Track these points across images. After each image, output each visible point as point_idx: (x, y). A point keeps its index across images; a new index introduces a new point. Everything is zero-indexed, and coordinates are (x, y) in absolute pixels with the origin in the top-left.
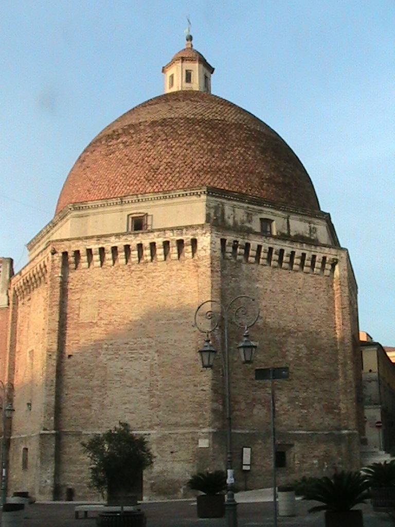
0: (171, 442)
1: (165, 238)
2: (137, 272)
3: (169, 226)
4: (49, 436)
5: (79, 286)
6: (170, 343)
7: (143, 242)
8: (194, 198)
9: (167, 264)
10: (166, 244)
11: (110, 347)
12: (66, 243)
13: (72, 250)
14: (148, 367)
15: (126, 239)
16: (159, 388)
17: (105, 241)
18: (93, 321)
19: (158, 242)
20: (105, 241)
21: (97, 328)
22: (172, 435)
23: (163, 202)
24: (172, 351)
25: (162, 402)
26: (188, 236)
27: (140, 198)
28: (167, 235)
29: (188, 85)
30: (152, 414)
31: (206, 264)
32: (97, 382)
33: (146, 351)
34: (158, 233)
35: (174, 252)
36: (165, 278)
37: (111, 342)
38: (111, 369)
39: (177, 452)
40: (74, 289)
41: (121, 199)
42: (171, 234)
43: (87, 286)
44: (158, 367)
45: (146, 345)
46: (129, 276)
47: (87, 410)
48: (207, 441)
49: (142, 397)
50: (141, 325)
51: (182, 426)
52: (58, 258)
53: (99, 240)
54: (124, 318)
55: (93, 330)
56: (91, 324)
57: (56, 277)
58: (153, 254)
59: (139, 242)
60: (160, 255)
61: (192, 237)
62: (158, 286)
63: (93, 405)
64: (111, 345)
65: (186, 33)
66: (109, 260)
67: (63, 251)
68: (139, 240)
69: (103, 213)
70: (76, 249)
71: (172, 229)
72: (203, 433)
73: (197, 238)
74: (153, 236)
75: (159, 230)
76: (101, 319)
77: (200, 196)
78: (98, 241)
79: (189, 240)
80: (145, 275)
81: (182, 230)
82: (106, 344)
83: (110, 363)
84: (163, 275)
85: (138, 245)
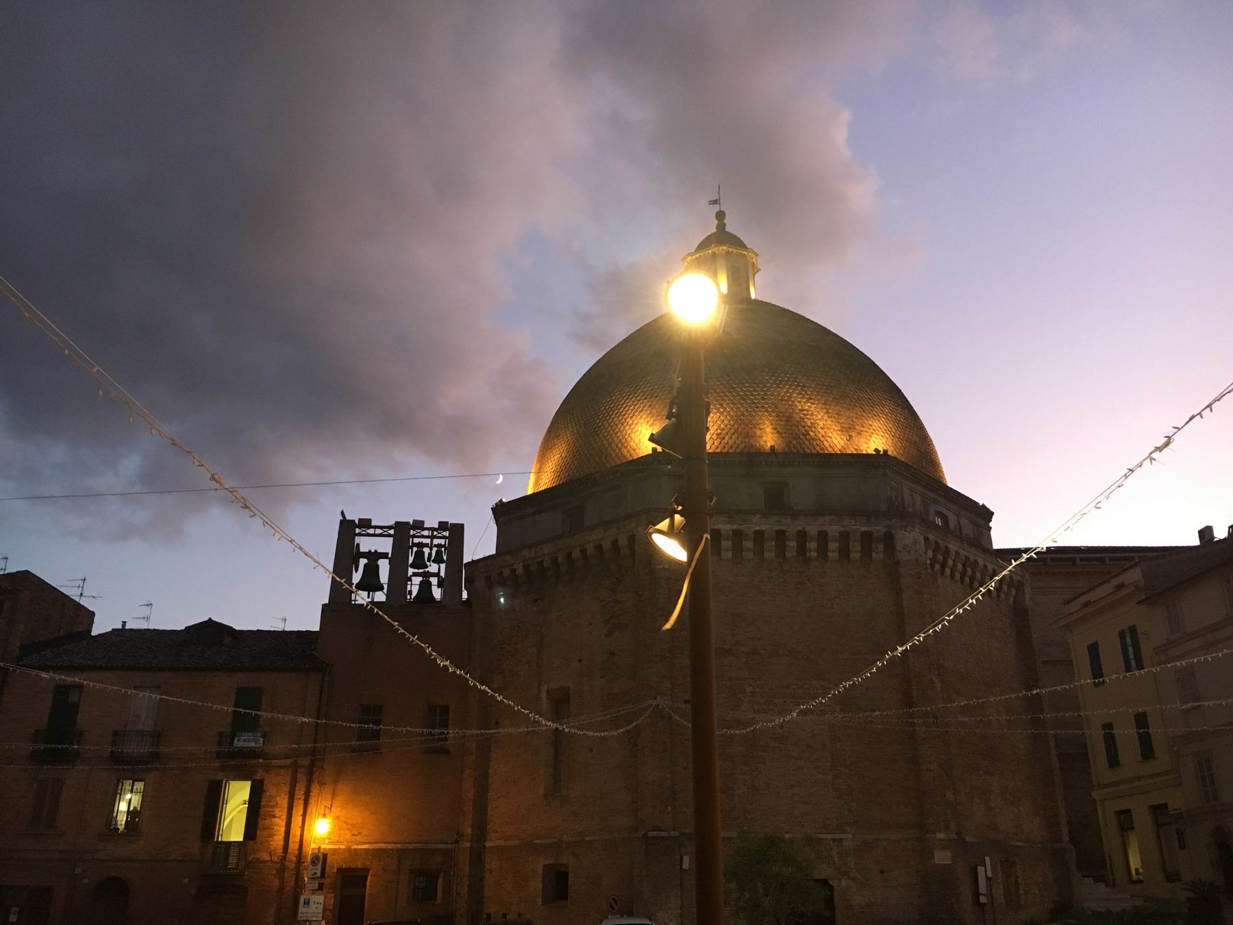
1: (844, 526)
7: (808, 528)
10: (845, 536)
11: (757, 690)
15: (779, 521)
18: (724, 646)
26: (879, 528)
48: (948, 853)
53: (732, 517)
57: (660, 569)
58: (823, 551)
60: (833, 551)
61: (884, 530)
73: (893, 531)
80: (808, 580)
82: (750, 685)
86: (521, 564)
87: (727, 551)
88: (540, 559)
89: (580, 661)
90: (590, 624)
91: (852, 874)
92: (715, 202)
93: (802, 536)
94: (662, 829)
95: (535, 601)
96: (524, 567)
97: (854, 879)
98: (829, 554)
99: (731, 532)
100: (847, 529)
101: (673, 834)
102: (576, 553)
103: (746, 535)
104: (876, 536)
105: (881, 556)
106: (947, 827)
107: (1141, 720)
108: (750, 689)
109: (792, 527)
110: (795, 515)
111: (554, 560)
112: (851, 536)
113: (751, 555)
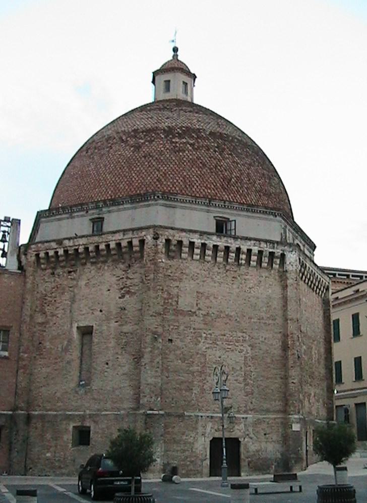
0: (264, 426)
1: (260, 247)
2: (232, 272)
3: (252, 236)
4: (158, 416)
5: (177, 275)
6: (261, 340)
7: (242, 247)
8: (271, 217)
9: (257, 270)
10: (260, 253)
11: (209, 336)
12: (171, 231)
13: (175, 238)
14: (243, 358)
16: (252, 377)
17: (208, 238)
18: (192, 310)
19: (254, 250)
20: (208, 238)
21: (196, 317)
22: (265, 420)
23: (245, 213)
24: (264, 347)
25: (256, 391)
26: (278, 251)
27: (226, 204)
28: (261, 246)
29: (184, 96)
30: (246, 400)
31: (293, 277)
32: (197, 368)
33: (240, 344)
34: (255, 242)
35: (265, 261)
36: (255, 282)
37: (210, 332)
38: (210, 357)
39: (268, 434)
40: (173, 276)
41: (210, 201)
42: (265, 246)
43: (185, 276)
44: (251, 360)
45: (241, 338)
46: (225, 275)
47: (187, 393)
48: (299, 425)
49: (238, 384)
50: (236, 320)
51: (272, 412)
52: (161, 244)
54: (221, 312)
55: (192, 318)
56: (190, 312)
57: (160, 262)
58: (248, 260)
59: (237, 246)
60: (254, 261)
61: (281, 252)
62: (250, 288)
63: (194, 388)
64: (209, 334)
65: (172, 45)
66: (209, 256)
67: (166, 238)
68: (238, 244)
69: (192, 209)
70: (180, 239)
71: (266, 241)
72: (295, 418)
73: (285, 253)
74: (250, 243)
75: (256, 240)
76: (199, 309)
77: (276, 216)
78: (201, 237)
79: (280, 254)
80: (239, 276)
81: (273, 244)
82: (204, 333)
83: (209, 351)
84: (254, 279)
85: (237, 248)
86: (62, 249)
87: (197, 254)
88: (77, 247)
89: (101, 311)
90: (109, 290)
91: (250, 435)
92: (173, 41)
93: (238, 250)
94: (155, 409)
95: (70, 272)
96: (64, 251)
97: (251, 438)
98: (251, 262)
99: (200, 244)
100: (262, 249)
101: (161, 412)
102: (102, 246)
103: (209, 247)
104: (276, 255)
105: (278, 266)
106: (299, 412)
107: (358, 361)
108: (205, 335)
109: (234, 245)
110: (235, 238)
111: (87, 249)
112: (264, 253)
113: (210, 258)
